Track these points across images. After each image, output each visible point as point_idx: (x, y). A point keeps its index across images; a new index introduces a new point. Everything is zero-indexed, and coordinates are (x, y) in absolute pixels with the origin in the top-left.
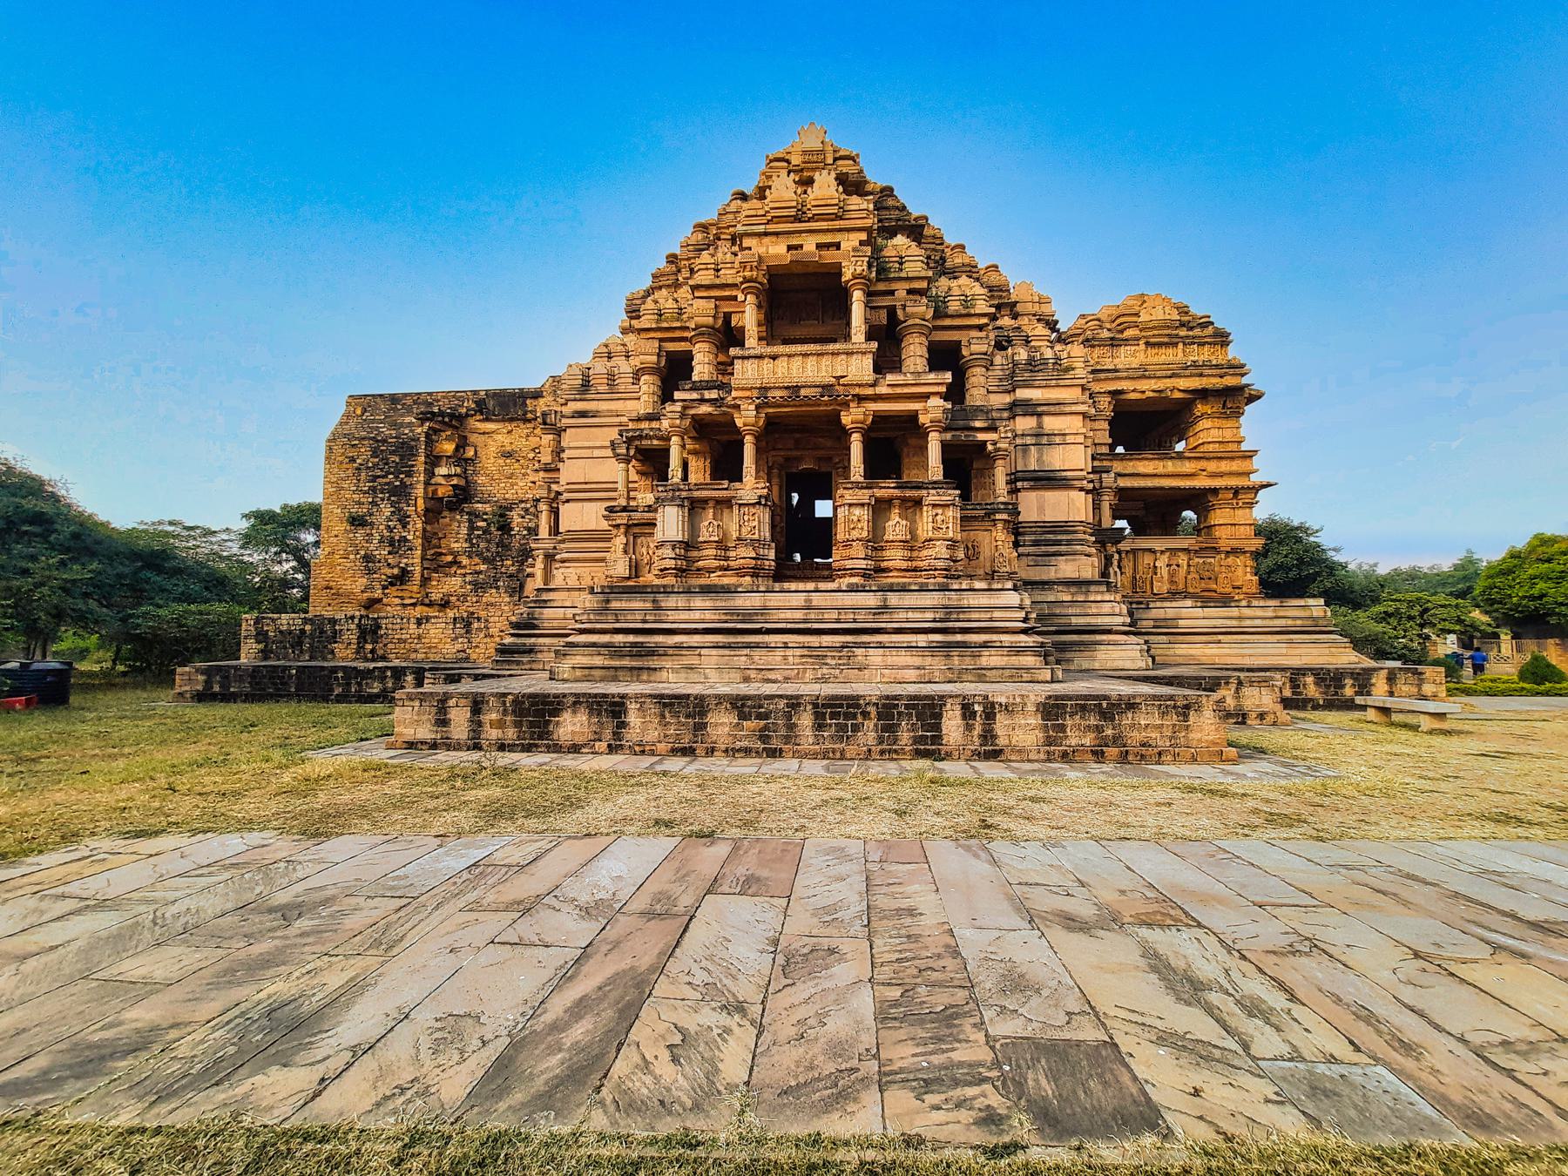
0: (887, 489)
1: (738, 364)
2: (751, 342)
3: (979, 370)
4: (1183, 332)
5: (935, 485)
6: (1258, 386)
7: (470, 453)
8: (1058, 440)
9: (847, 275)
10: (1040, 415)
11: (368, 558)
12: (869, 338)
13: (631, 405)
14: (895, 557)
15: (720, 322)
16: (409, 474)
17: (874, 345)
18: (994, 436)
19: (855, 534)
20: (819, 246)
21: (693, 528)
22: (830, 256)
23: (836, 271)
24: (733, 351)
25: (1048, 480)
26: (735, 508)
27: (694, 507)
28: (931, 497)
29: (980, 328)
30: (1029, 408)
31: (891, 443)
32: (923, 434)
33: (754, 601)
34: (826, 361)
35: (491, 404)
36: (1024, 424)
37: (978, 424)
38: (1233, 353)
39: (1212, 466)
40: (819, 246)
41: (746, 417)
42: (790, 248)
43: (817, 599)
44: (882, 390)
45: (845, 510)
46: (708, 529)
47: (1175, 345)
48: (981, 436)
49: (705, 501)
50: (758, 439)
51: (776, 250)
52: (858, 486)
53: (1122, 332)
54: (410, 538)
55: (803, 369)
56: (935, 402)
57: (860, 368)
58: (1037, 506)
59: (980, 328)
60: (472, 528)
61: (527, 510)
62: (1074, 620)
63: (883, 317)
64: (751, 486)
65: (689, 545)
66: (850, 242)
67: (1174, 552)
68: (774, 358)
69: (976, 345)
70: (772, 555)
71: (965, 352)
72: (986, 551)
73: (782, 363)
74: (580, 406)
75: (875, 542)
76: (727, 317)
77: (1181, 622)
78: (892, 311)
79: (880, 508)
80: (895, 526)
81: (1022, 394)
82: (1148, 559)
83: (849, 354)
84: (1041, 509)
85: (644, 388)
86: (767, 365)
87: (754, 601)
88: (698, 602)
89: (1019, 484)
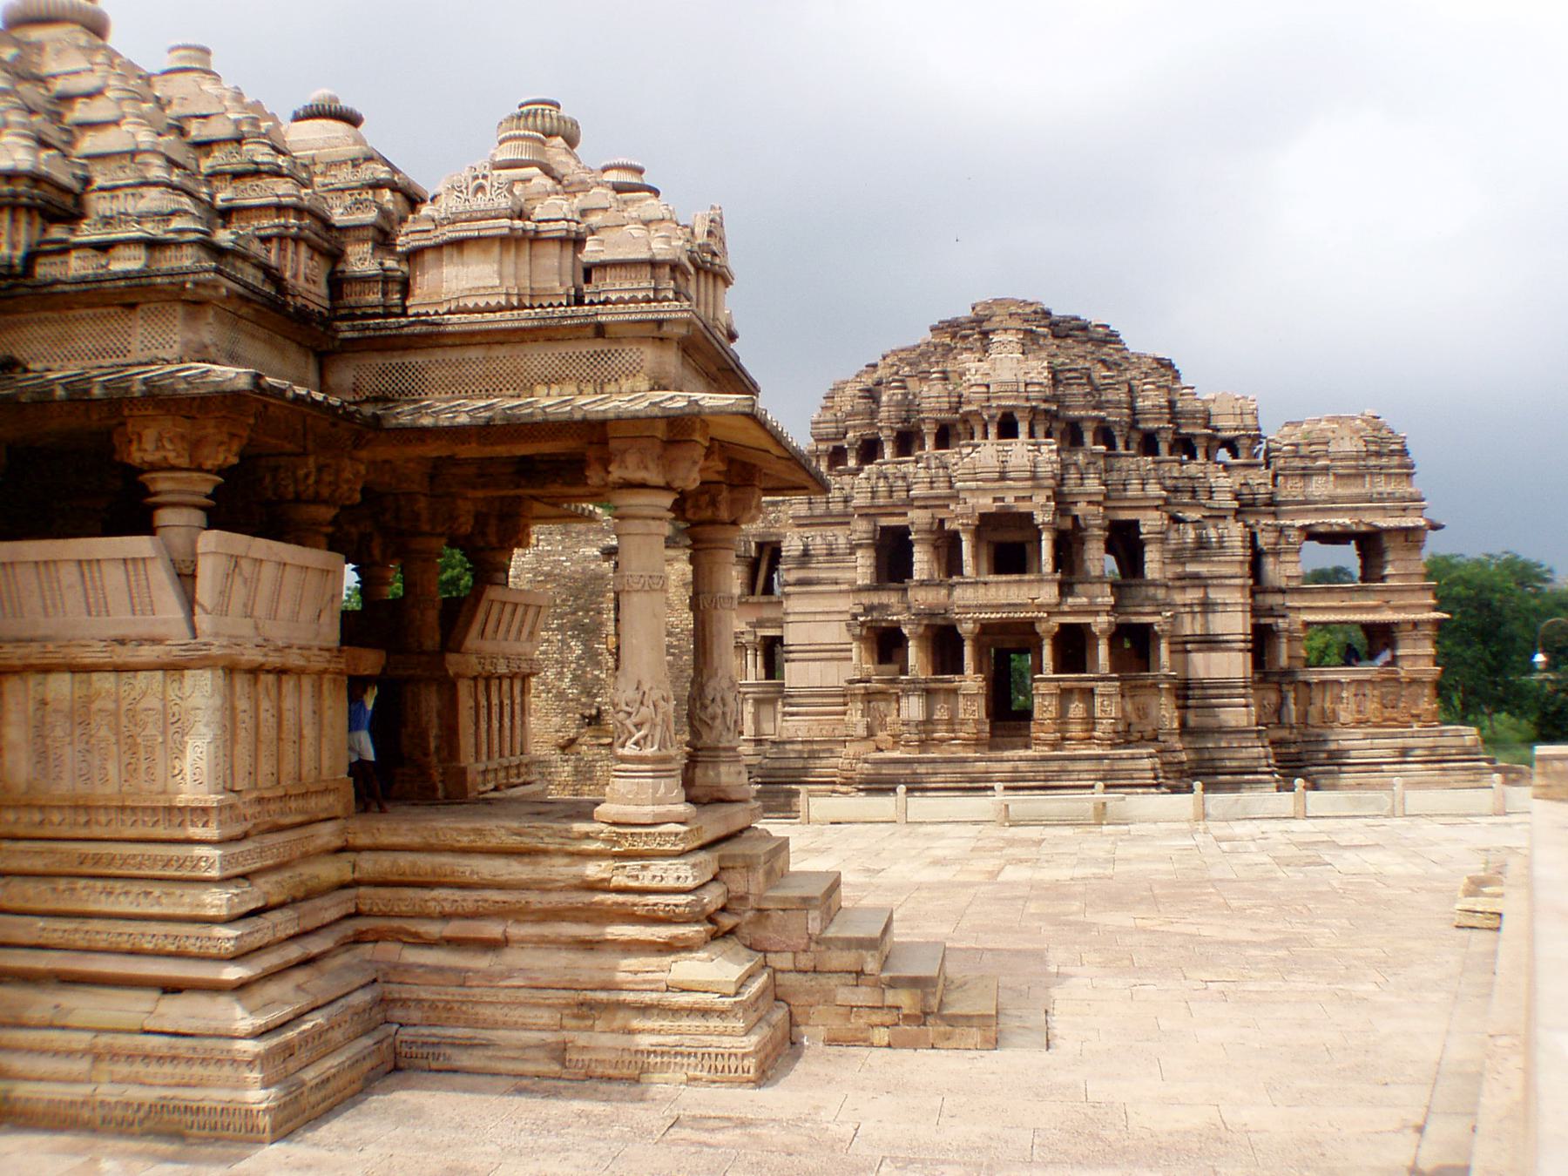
2: (968, 568)
4: (1372, 462)
5: (1102, 679)
6: (1438, 520)
8: (1220, 608)
9: (1039, 518)
10: (1206, 586)
11: (561, 695)
13: (849, 575)
14: (1076, 730)
15: (935, 526)
16: (600, 613)
17: (1058, 576)
18: (1158, 618)
19: (1046, 715)
20: (1017, 499)
21: (929, 711)
22: (1023, 507)
23: (1030, 516)
24: (955, 579)
25: (1210, 642)
26: (961, 698)
27: (929, 693)
28: (1100, 688)
30: (1198, 580)
31: (1073, 647)
34: (1025, 588)
36: (1193, 595)
38: (1416, 487)
39: (1396, 600)
40: (1017, 499)
41: (967, 628)
42: (995, 500)
44: (1066, 609)
45: (1044, 689)
46: (941, 713)
47: (1363, 476)
49: (936, 691)
51: (986, 503)
53: (1316, 458)
54: (603, 676)
57: (1049, 594)
58: (1205, 665)
62: (1228, 763)
64: (971, 681)
65: (929, 721)
66: (1040, 498)
67: (1360, 682)
68: (986, 583)
69: (1151, 522)
70: (987, 728)
71: (1143, 530)
73: (992, 591)
74: (802, 574)
75: (1062, 718)
76: (942, 521)
77: (1353, 753)
79: (1065, 695)
80: (1076, 709)
81: (1191, 568)
82: (1336, 690)
84: (1208, 667)
85: (860, 561)
86: (981, 590)
88: (943, 768)
89: (1189, 647)
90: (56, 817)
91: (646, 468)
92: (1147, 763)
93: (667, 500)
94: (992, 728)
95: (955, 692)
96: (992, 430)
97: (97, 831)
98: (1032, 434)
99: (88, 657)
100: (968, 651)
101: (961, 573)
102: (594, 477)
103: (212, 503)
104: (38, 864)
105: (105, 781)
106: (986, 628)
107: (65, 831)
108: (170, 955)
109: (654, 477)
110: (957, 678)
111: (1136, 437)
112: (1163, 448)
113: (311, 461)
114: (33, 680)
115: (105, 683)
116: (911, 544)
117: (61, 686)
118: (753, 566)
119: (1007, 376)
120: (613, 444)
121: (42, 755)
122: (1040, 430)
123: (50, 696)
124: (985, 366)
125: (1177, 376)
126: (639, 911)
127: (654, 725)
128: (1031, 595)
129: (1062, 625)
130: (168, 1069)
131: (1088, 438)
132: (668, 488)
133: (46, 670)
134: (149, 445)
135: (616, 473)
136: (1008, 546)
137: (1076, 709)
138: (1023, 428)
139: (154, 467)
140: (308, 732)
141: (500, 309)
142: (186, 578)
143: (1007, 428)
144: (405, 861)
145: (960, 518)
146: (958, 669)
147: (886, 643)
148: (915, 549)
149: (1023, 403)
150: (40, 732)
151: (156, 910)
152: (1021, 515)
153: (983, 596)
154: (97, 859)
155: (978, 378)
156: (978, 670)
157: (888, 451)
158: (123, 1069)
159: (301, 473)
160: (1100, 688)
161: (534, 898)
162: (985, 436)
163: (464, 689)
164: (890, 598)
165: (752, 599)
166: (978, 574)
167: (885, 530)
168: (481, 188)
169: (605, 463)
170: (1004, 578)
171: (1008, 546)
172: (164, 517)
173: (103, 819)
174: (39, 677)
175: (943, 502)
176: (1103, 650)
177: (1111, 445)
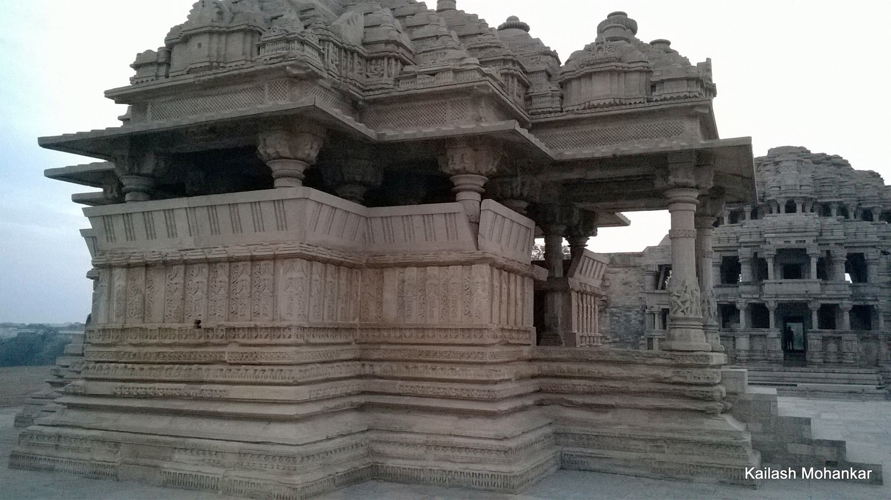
0: (828, 332)
1: (766, 286)
3: (872, 266)
7: (607, 284)
12: (818, 277)
18: (877, 303)
20: (797, 241)
22: (801, 246)
24: (764, 281)
29: (874, 247)
31: (829, 315)
32: (842, 311)
33: (780, 374)
34: (802, 285)
35: (618, 260)
37: (870, 298)
40: (797, 241)
41: (771, 305)
43: (803, 375)
48: (871, 303)
50: (775, 312)
51: (781, 243)
52: (816, 332)
55: (793, 289)
56: (845, 302)
59: (874, 247)
60: (611, 320)
61: (638, 312)
63: (824, 255)
64: (774, 332)
65: (751, 350)
66: (809, 241)
70: (782, 355)
72: (875, 352)
73: (784, 286)
75: (824, 351)
76: (756, 254)
78: (828, 252)
79: (825, 340)
80: (832, 347)
83: (812, 283)
86: (778, 286)
87: (780, 374)
90: (408, 334)
91: (688, 177)
92: (874, 376)
93: (695, 194)
94: (785, 356)
95: (765, 336)
96: (783, 209)
97: (427, 340)
98: (803, 211)
99: (427, 259)
100: (772, 316)
101: (767, 278)
102: (659, 184)
103: (484, 190)
104: (399, 356)
105: (432, 316)
106: (781, 306)
107: (412, 340)
108: (464, 399)
109: (693, 182)
110: (767, 330)
111: (860, 212)
112: (876, 217)
113: (519, 179)
114: (398, 271)
115: (433, 271)
116: (740, 265)
117: (412, 273)
118: (657, 276)
119: (790, 182)
120: (670, 167)
121: (401, 306)
122: (808, 208)
123: (406, 277)
124: (778, 178)
125: (882, 180)
126: (687, 394)
127: (692, 302)
128: (807, 287)
129: (823, 306)
130: (464, 454)
131: (834, 212)
132: (697, 187)
133: (405, 265)
134: (457, 159)
135: (672, 180)
136: (792, 265)
137: (832, 347)
138: (799, 208)
139: (458, 172)
140: (520, 303)
141: (611, 105)
142: (475, 224)
143: (791, 208)
144: (564, 366)
145: (768, 252)
146: (767, 326)
147: (728, 312)
148: (742, 266)
149: (798, 195)
150: (401, 294)
151: (456, 377)
152: (801, 250)
153: (778, 289)
154: (428, 353)
155: (775, 184)
156: (776, 325)
157: (726, 219)
158: (441, 453)
159: (514, 185)
160: (845, 337)
161: (632, 386)
162: (779, 211)
163: (574, 295)
164: (728, 290)
165: (656, 291)
166: (775, 278)
167: (725, 259)
168: (600, 48)
169: (665, 177)
170: (790, 280)
171: (792, 265)
172: (461, 196)
173: (430, 335)
174: (401, 270)
175: (756, 245)
176: (847, 317)
177: (847, 216)
